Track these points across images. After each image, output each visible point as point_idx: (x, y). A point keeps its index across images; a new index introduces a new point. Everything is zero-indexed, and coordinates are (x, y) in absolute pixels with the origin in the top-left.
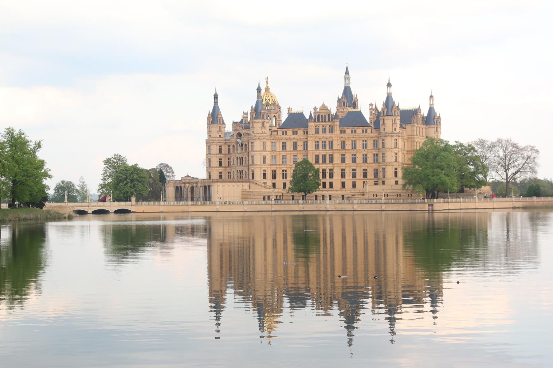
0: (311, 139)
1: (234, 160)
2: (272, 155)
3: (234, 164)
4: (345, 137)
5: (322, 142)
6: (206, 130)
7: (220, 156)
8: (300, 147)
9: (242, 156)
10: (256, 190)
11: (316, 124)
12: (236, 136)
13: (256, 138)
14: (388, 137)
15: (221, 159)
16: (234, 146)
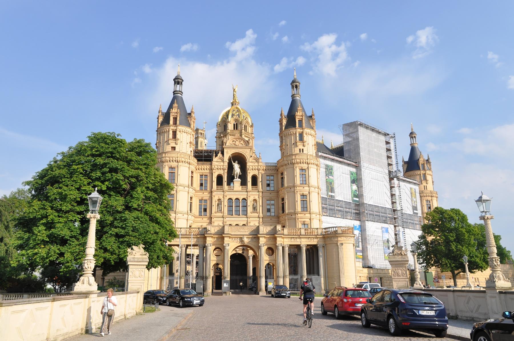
9: (245, 197)
12: (230, 160)
16: (220, 179)
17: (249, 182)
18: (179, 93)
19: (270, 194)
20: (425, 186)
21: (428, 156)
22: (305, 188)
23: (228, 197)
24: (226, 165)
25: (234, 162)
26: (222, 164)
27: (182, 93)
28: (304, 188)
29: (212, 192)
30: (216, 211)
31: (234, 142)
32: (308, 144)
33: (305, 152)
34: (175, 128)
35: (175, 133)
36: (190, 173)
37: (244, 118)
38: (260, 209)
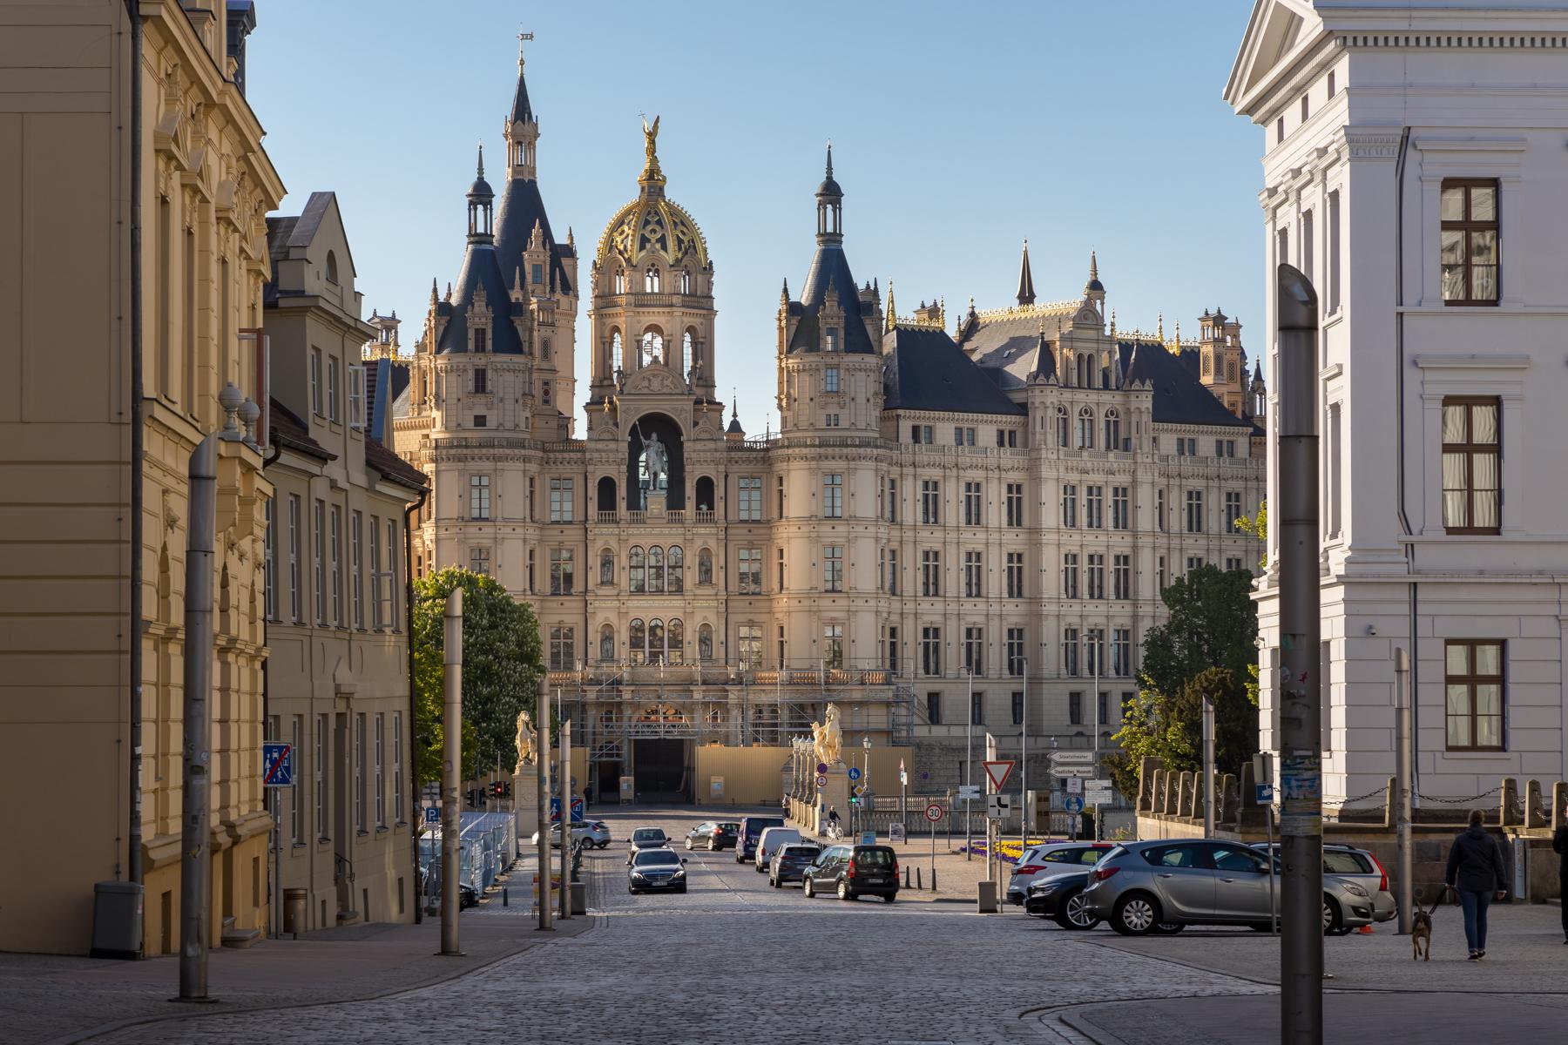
1: (607, 563)
9: (679, 541)
12: (633, 431)
16: (607, 486)
17: (689, 498)
18: (485, 243)
19: (750, 531)
23: (633, 542)
25: (648, 437)
26: (612, 445)
28: (833, 528)
29: (586, 529)
30: (599, 581)
31: (646, 383)
33: (843, 423)
34: (483, 361)
35: (480, 376)
36: (528, 483)
37: (680, 249)
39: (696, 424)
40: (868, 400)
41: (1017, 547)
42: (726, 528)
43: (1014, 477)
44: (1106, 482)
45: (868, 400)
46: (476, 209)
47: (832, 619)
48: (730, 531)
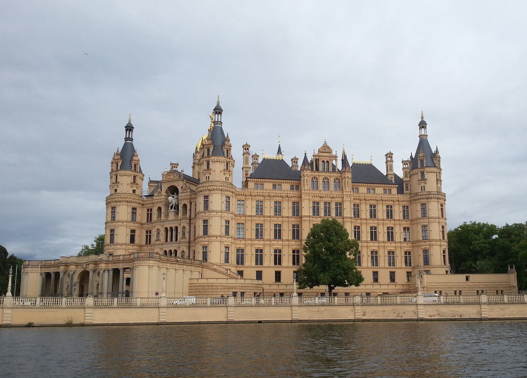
0: (308, 197)
1: (158, 233)
2: (238, 222)
3: (158, 240)
4: (361, 198)
5: (325, 203)
6: (107, 182)
7: (133, 226)
8: (287, 209)
10: (220, 281)
11: (313, 173)
12: (166, 192)
13: (214, 187)
14: (433, 200)
15: (133, 231)
16: (160, 209)
20: (423, 187)
21: (437, 149)
22: (207, 214)
24: (163, 199)
25: (173, 194)
27: (133, 139)
28: (205, 214)
31: (169, 177)
32: (214, 171)
38: (187, 235)
39: (182, 187)
40: (221, 171)
41: (296, 223)
42: (190, 220)
43: (294, 199)
44: (332, 201)
45: (221, 171)
46: (130, 133)
47: (204, 244)
48: (192, 221)
